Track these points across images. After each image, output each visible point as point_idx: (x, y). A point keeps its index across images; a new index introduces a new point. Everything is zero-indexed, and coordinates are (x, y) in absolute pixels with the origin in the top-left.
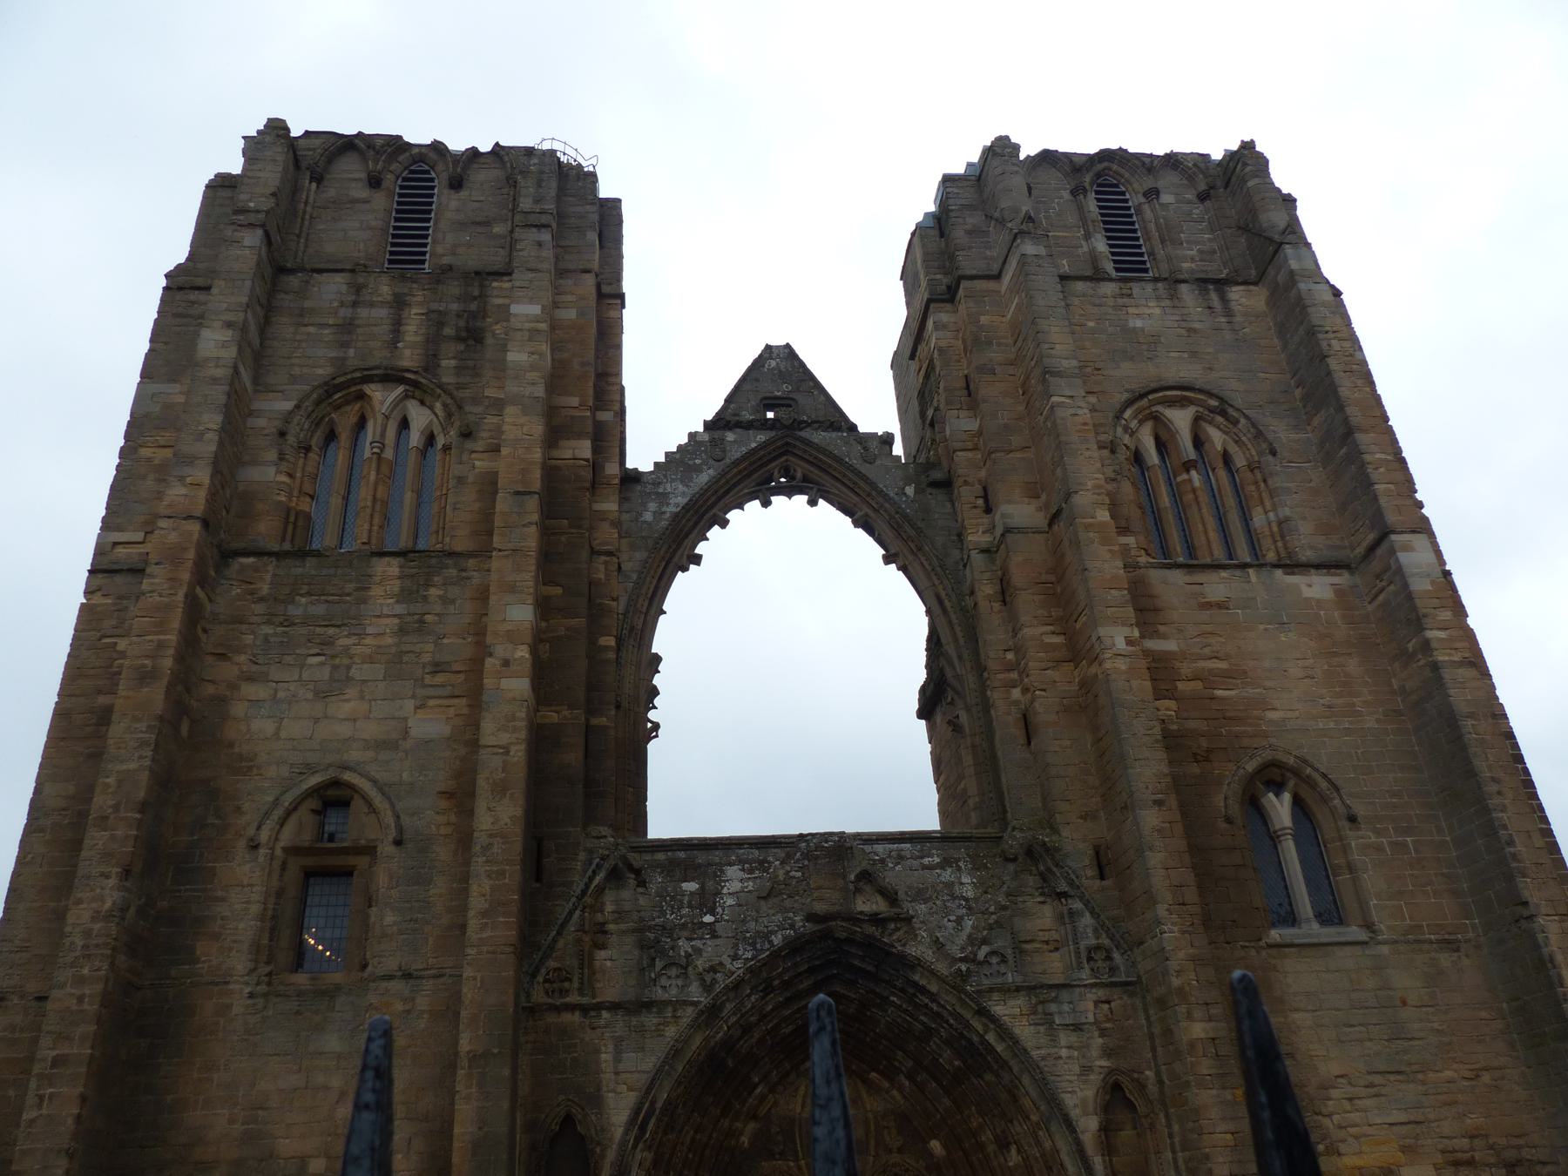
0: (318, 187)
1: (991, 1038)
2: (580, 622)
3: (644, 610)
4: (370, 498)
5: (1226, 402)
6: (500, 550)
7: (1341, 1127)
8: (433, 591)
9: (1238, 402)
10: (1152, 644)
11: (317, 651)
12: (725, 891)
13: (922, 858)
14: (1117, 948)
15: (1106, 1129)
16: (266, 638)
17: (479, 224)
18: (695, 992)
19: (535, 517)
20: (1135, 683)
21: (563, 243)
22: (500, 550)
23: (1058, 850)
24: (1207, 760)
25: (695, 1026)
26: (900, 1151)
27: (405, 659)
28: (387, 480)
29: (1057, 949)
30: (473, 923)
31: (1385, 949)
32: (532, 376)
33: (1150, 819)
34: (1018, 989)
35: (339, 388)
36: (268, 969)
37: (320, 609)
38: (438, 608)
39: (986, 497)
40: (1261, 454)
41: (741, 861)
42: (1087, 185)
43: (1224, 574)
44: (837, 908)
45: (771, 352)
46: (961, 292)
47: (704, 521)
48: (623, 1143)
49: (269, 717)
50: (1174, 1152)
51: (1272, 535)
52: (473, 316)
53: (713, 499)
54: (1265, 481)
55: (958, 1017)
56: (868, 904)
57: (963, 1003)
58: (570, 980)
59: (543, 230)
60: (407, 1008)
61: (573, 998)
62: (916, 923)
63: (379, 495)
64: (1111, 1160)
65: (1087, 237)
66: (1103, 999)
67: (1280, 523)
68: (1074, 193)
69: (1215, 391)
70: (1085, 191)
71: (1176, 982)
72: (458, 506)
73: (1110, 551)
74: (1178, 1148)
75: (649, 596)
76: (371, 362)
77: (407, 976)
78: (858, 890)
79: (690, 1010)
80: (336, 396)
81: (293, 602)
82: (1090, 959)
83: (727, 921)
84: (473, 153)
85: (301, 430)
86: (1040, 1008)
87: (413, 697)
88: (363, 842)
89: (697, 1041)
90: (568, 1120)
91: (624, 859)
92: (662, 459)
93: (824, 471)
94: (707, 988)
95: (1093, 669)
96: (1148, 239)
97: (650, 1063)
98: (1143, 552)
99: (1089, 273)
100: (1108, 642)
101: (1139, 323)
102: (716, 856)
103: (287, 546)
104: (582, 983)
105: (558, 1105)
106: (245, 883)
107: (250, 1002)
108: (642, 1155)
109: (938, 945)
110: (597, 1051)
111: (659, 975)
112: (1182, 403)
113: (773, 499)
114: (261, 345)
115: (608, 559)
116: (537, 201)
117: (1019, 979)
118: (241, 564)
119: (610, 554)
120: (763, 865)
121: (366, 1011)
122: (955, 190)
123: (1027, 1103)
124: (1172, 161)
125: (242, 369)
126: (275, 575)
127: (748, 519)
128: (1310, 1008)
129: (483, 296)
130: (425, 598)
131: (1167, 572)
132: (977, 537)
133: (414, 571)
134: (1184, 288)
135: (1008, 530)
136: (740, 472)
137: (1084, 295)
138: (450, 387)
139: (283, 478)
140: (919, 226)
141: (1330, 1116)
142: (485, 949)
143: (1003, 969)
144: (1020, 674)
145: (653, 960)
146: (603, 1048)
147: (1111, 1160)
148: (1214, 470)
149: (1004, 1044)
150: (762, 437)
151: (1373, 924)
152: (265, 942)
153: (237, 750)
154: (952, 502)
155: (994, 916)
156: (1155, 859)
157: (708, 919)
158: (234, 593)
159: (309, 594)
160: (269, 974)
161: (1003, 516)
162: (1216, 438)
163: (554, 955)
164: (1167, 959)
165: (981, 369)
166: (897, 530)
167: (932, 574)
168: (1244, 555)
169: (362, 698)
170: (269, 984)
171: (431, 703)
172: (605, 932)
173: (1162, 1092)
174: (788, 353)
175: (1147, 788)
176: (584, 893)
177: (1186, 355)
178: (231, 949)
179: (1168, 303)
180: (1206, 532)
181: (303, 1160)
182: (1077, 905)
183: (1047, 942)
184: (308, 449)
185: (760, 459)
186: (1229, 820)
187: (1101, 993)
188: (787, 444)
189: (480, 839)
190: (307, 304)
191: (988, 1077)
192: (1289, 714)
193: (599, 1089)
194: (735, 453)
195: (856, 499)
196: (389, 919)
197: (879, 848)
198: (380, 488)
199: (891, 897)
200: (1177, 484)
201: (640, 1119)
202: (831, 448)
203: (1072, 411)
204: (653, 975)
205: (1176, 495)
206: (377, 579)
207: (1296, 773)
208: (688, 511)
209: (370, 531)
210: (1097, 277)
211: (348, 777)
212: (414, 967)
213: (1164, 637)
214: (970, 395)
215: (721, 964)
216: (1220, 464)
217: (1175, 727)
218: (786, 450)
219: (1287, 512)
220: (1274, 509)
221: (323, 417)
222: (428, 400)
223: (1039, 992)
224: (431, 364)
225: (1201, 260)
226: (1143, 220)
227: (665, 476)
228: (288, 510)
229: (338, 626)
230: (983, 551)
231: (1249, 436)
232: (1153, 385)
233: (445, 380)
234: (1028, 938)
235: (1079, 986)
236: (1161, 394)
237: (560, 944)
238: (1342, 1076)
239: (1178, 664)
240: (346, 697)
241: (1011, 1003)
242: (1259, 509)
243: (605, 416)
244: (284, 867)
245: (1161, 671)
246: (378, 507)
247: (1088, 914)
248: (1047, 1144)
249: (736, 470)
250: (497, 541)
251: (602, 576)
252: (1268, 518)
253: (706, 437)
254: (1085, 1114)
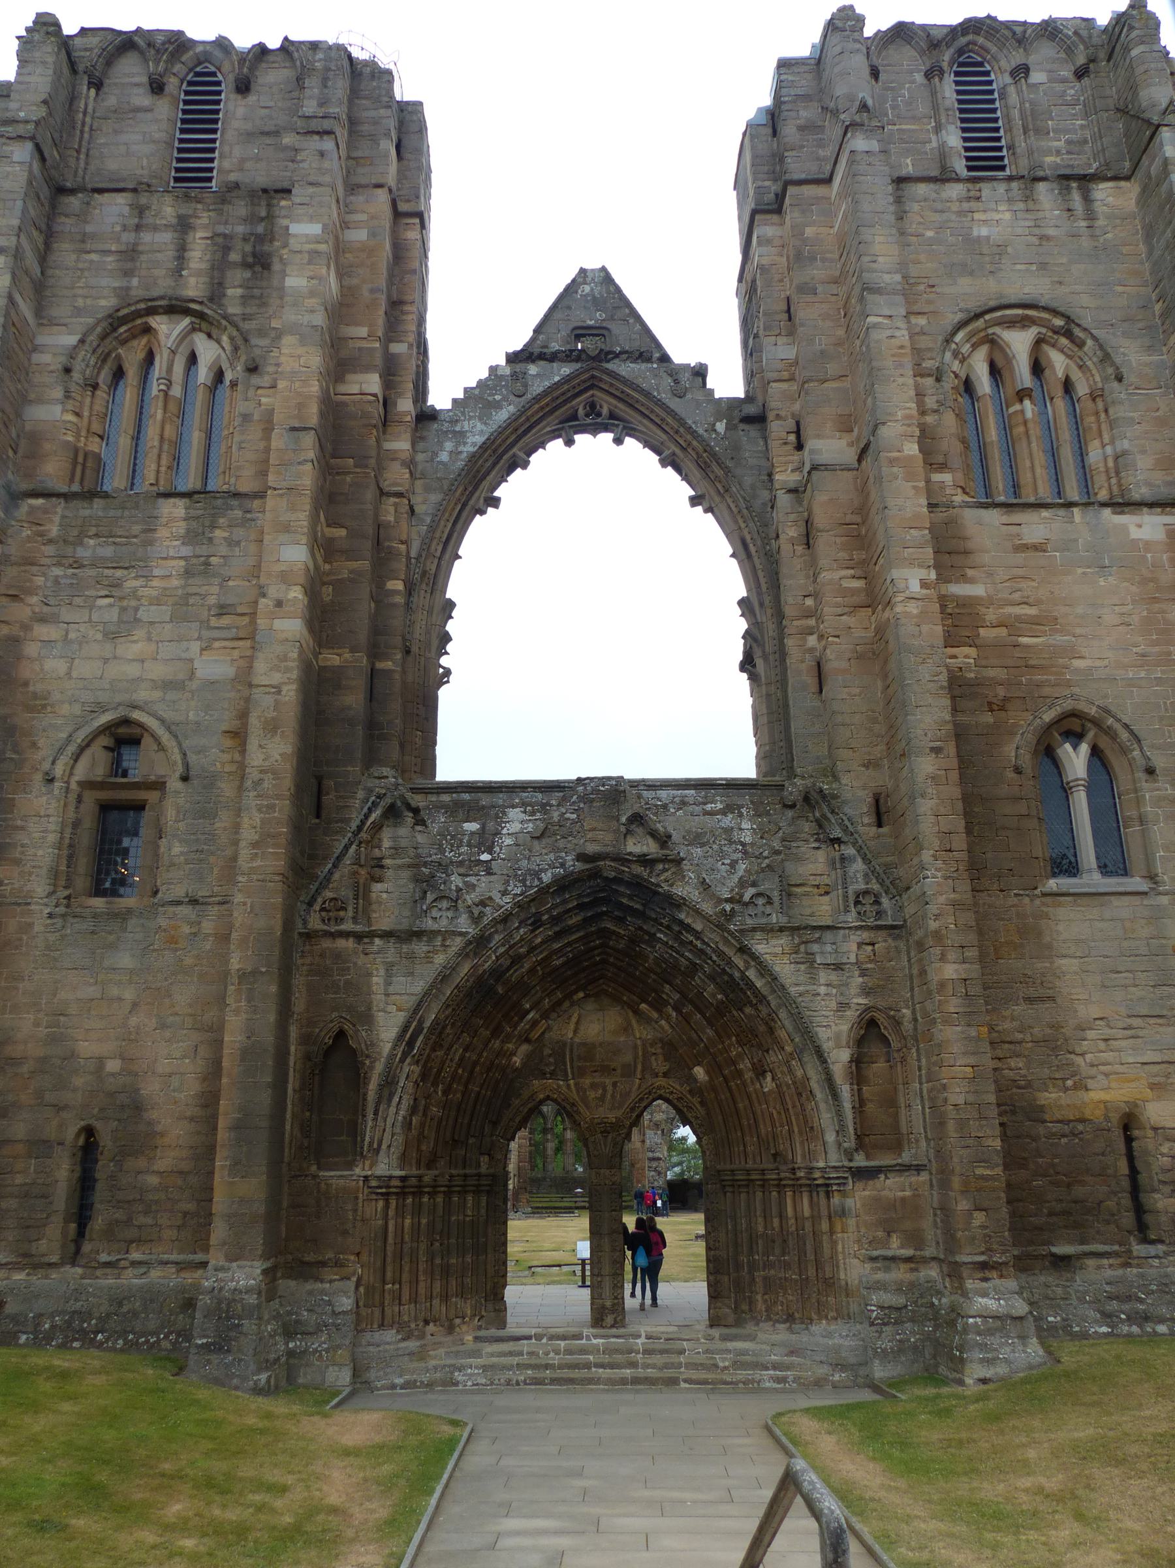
0: (97, 94)
1: (751, 974)
2: (364, 565)
3: (438, 554)
4: (157, 438)
5: (1073, 321)
6: (275, 489)
7: (1092, 1066)
8: (218, 533)
9: (1087, 322)
10: (957, 589)
11: (107, 593)
12: (505, 831)
13: (705, 804)
14: (886, 893)
15: (858, 1062)
16: (56, 581)
17: (267, 134)
18: (464, 923)
19: (311, 455)
20: (925, 628)
21: (355, 154)
22: (275, 489)
23: (835, 797)
24: (1002, 708)
25: (463, 954)
26: (665, 1075)
27: (191, 601)
28: (175, 419)
29: (827, 893)
30: (244, 853)
31: (1165, 900)
32: (312, 302)
33: (926, 766)
34: (781, 930)
35: (124, 320)
36: (67, 893)
37: (108, 551)
38: (223, 550)
39: (798, 433)
40: (1105, 379)
41: (524, 804)
42: (945, 65)
43: (1045, 513)
44: (609, 849)
45: (586, 276)
46: (787, 201)
47: (502, 462)
48: (391, 1056)
49: (62, 657)
50: (921, 1083)
51: (1107, 471)
52: (260, 239)
53: (513, 437)
54: (1106, 411)
55: (721, 954)
57: (726, 941)
58: (345, 909)
59: (325, 137)
60: (193, 930)
61: (347, 926)
62: (686, 865)
63: (167, 434)
64: (859, 1090)
65: (938, 129)
66: (867, 941)
67: (1117, 458)
68: (928, 75)
69: (1061, 309)
70: (942, 72)
71: (933, 925)
72: (243, 445)
73: (914, 487)
74: (924, 1080)
75: (444, 539)
76: (156, 293)
77: (194, 902)
78: (629, 832)
79: (458, 940)
80: (122, 330)
81: (81, 544)
82: (857, 903)
83: (503, 859)
84: (261, 51)
85: (87, 366)
86: (802, 948)
87: (199, 638)
88: (153, 778)
89: (465, 968)
90: (341, 1035)
91: (402, 797)
92: (461, 395)
93: (631, 406)
94: (476, 920)
95: (887, 614)
96: (1009, 130)
97: (419, 987)
98: (959, 490)
99: (935, 173)
100: (902, 585)
101: (984, 232)
102: (500, 799)
103: (76, 488)
104: (356, 913)
105: (332, 1021)
106: (42, 814)
107: (49, 921)
108: (409, 1069)
109: (705, 886)
110: (370, 975)
111: (430, 908)
112: (1023, 323)
113: (577, 437)
114: (42, 273)
115: (397, 500)
116: (321, 105)
117: (783, 920)
118: (31, 506)
119: (400, 495)
120: (544, 808)
121: (156, 933)
122: (791, 78)
123: (782, 1034)
125: (18, 298)
126: (63, 517)
128: (1078, 954)
129: (270, 218)
130: (210, 539)
131: (983, 512)
132: (785, 476)
133: (201, 512)
134: (1042, 187)
135: (814, 468)
136: (542, 408)
137: (925, 200)
138: (235, 318)
139: (70, 417)
140: (750, 125)
141: (1082, 1055)
142: (255, 877)
143: (768, 910)
144: (817, 620)
145: (425, 892)
146: (375, 973)
147: (859, 1090)
148: (1052, 399)
149: (764, 981)
150: (566, 370)
151: (1157, 875)
152: (63, 868)
153: (31, 688)
154: (765, 439)
155: (767, 861)
156: (926, 806)
157: (485, 857)
158: (24, 534)
159: (97, 535)
160: (68, 898)
161: (812, 452)
162: (1058, 362)
163: (331, 886)
164: (927, 903)
165: (803, 289)
166: (704, 467)
167: (739, 518)
168: (1073, 492)
169: (149, 639)
170: (68, 906)
171: (217, 644)
172: (382, 867)
173: (915, 1029)
174: (605, 277)
175: (926, 735)
176: (360, 828)
177: (1034, 267)
178: (30, 874)
179: (1021, 206)
180: (1033, 468)
181: (101, 1061)
182: (850, 851)
183: (818, 886)
184: (95, 387)
185: (563, 394)
186: (1018, 770)
187: (865, 936)
188: (593, 377)
189: (253, 774)
190: (89, 229)
191: (748, 1010)
192: (1098, 663)
193: (370, 1009)
194: (537, 388)
195: (664, 437)
196: (177, 849)
197: (663, 794)
198: (168, 427)
199: (664, 840)
200: (1010, 416)
201: (408, 1036)
202: (639, 381)
203: (889, 333)
204: (424, 907)
205: (1006, 428)
206: (164, 520)
207: (1096, 723)
208: (486, 450)
209: (158, 472)
210: (944, 177)
211: (136, 715)
212: (200, 894)
213: (971, 581)
214: (790, 319)
215: (490, 898)
216: (1059, 392)
217: (972, 675)
218: (592, 384)
219: (1126, 444)
220: (1112, 442)
221: (109, 354)
222: (215, 332)
224: (216, 294)
225: (1068, 153)
226: (1006, 106)
227: (463, 413)
228: (76, 451)
229: (126, 568)
230: (790, 491)
231: (1095, 359)
232: (992, 303)
233: (231, 310)
234: (799, 882)
235: (844, 928)
236: (999, 314)
237: (336, 876)
238: (1101, 1019)
239: (984, 610)
240: (135, 638)
241: (774, 942)
242: (1097, 443)
244: (79, 800)
246: (166, 447)
247: (860, 860)
248: (799, 1073)
249: (537, 406)
250: (272, 479)
251: (392, 519)
252: (1104, 453)
253: (508, 371)
254: (838, 1046)
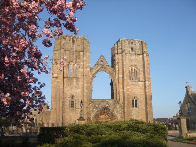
127: (99, 73)
150: (101, 66)
162: (136, 69)
194: (99, 68)
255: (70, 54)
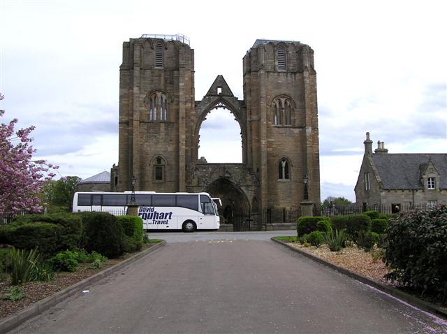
10: (270, 140)
56: (227, 175)
124: (293, 44)
127: (214, 112)
150: (217, 98)
162: (288, 103)
223: (247, 186)
243: (192, 96)
245: (269, 144)
255: (153, 76)
